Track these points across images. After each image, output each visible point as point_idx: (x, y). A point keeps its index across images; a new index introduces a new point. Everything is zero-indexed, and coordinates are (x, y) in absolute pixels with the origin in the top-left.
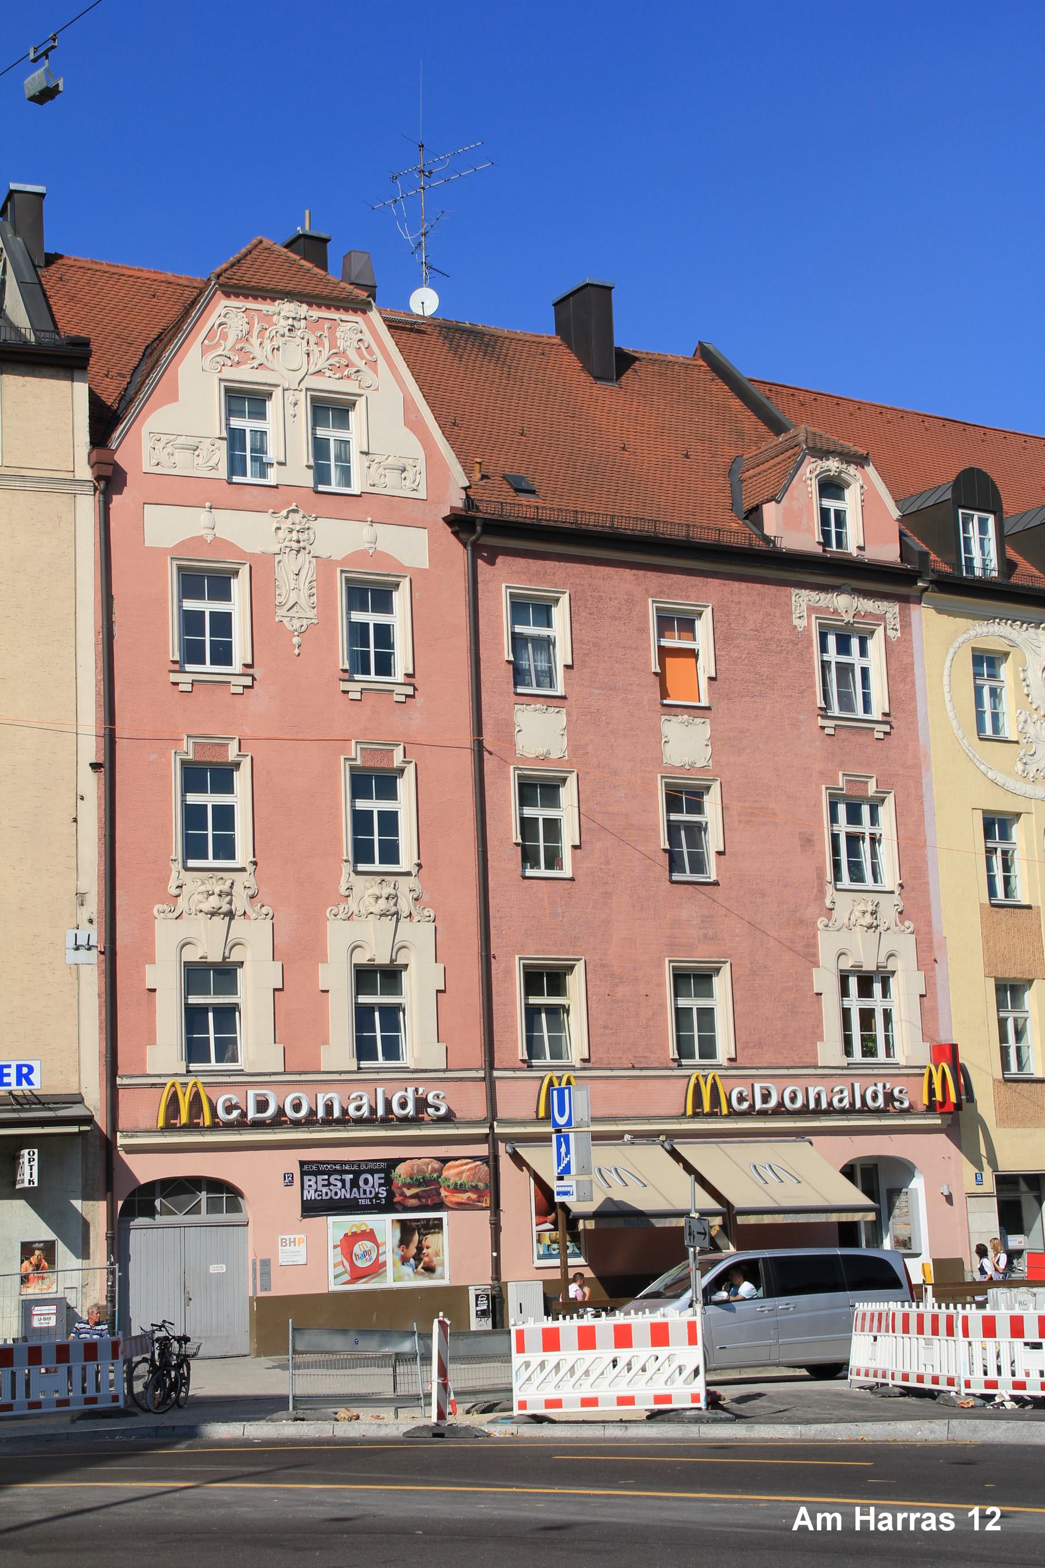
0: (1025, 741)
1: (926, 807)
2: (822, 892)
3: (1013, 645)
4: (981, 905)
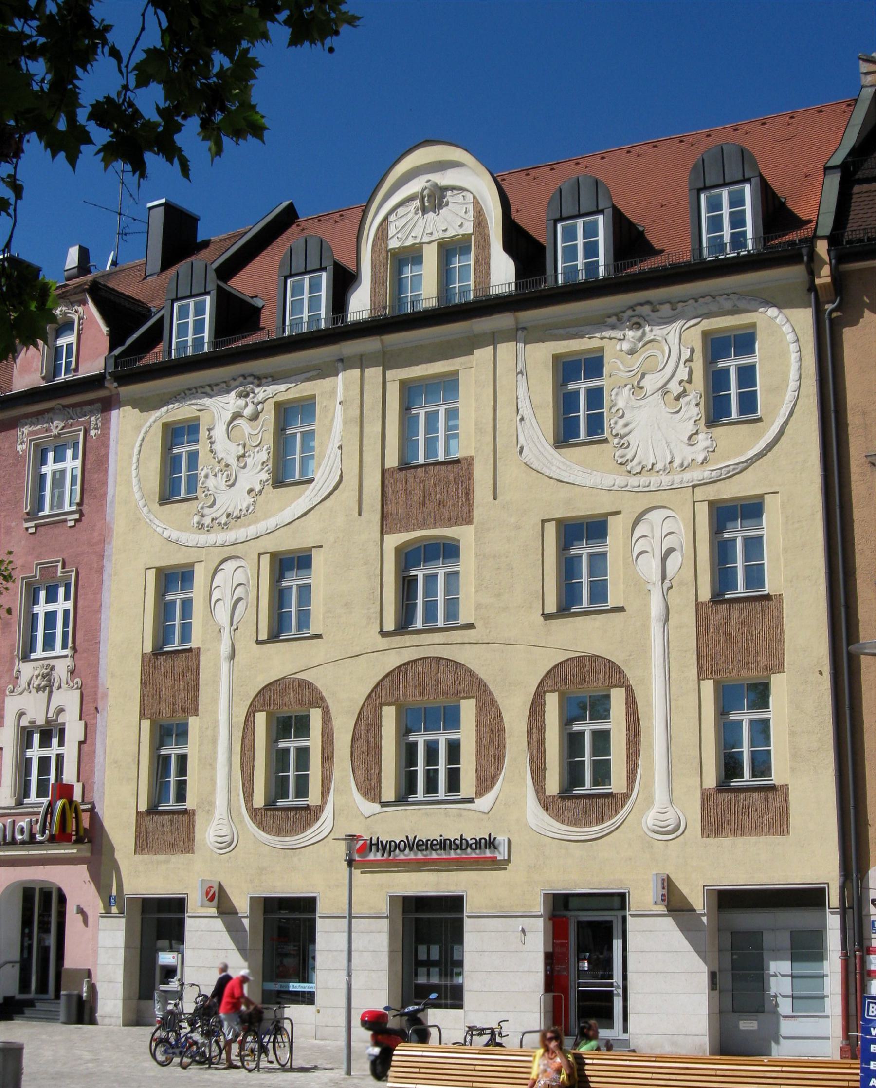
0: (204, 494)
1: (106, 576)
2: (12, 664)
3: (202, 408)
4: (144, 655)
